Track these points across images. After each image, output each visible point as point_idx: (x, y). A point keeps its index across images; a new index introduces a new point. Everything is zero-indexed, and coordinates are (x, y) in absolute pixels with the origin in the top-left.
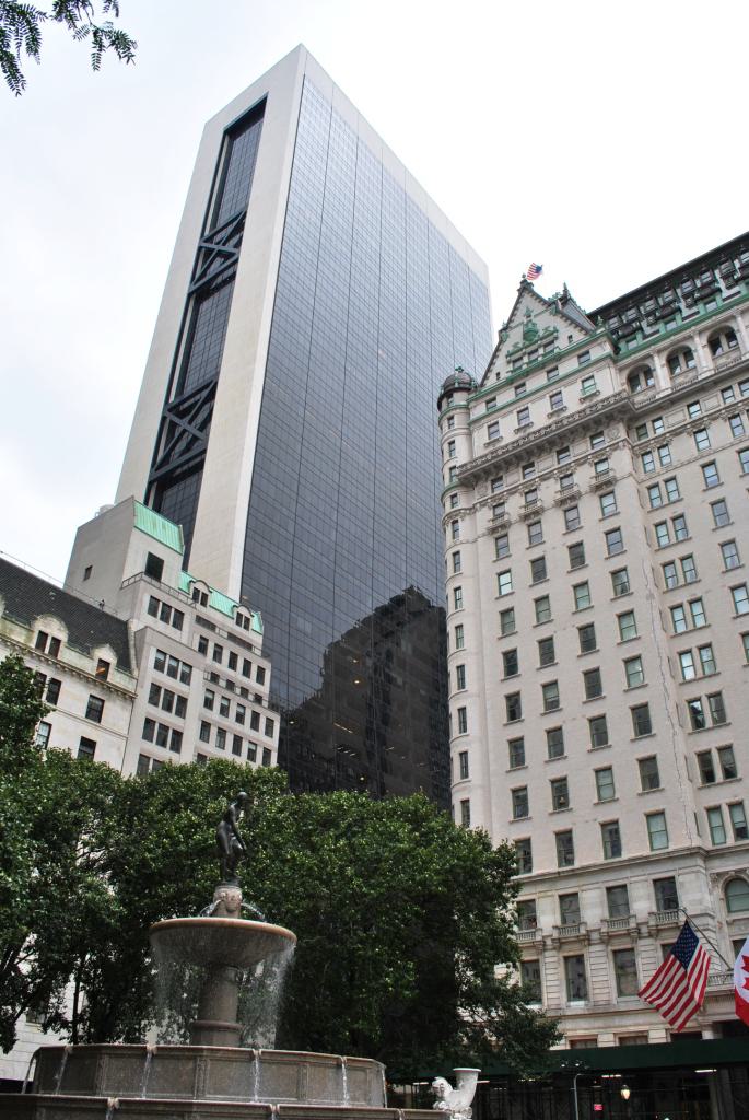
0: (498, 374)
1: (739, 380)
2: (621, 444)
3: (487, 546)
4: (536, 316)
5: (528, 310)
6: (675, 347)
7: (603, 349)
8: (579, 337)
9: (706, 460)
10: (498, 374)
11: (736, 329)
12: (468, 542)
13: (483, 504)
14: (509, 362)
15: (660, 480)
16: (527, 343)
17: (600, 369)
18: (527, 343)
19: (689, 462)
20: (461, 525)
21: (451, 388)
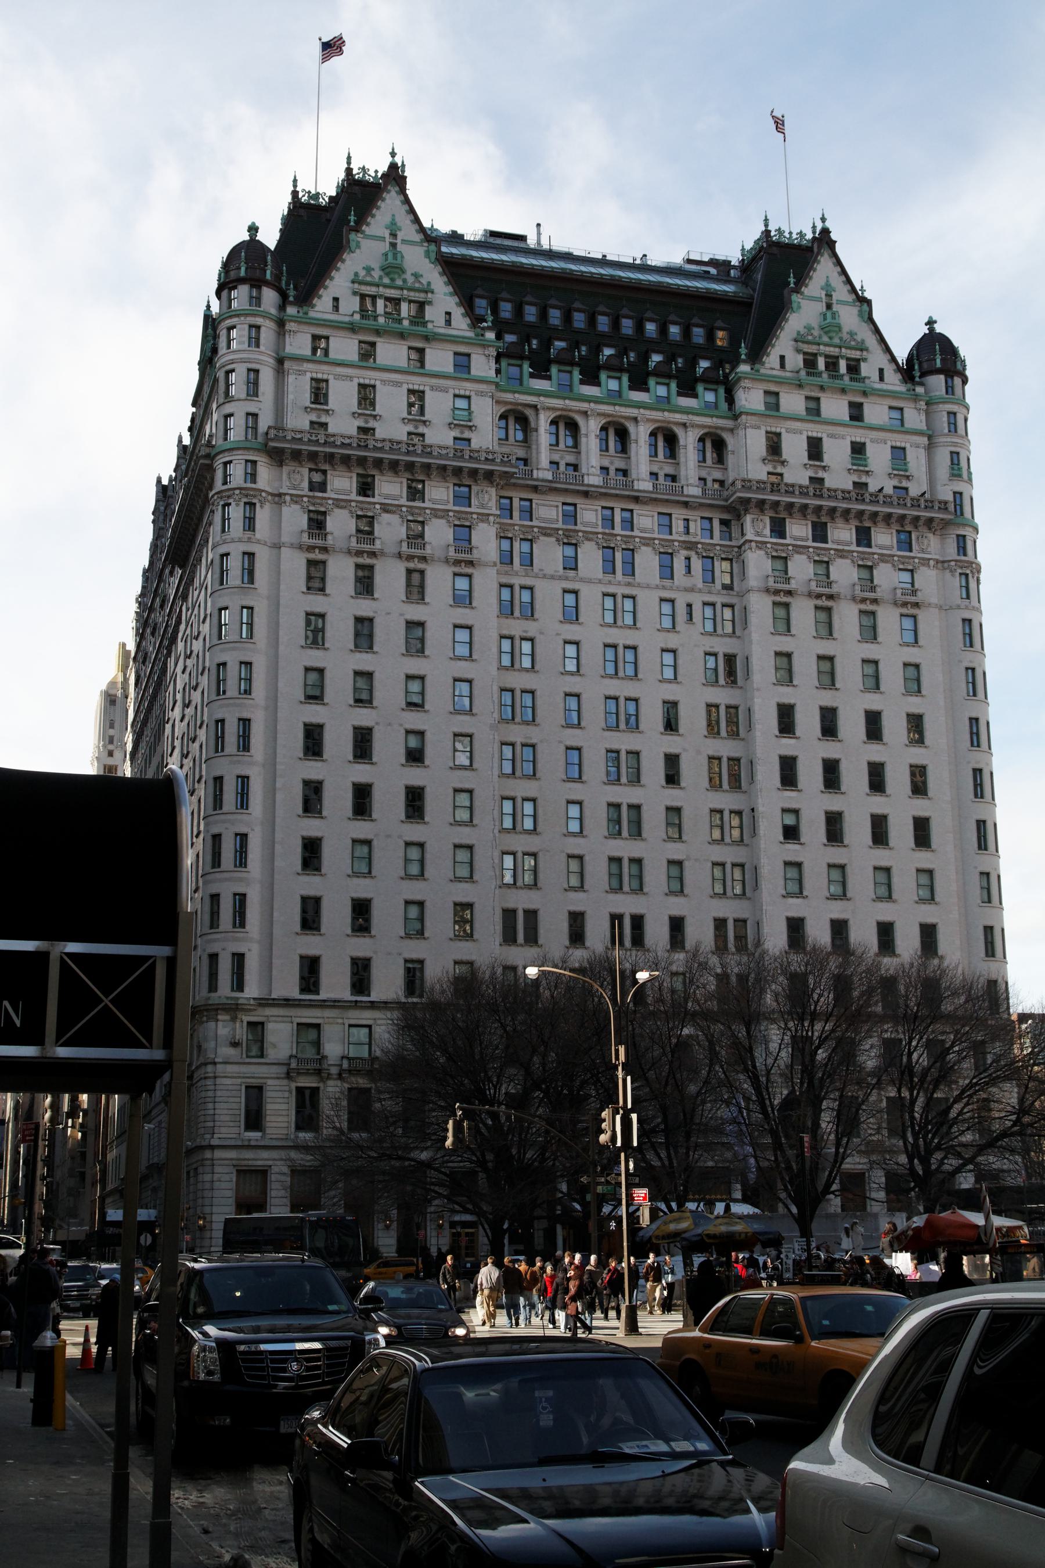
0: (336, 300)
1: (624, 507)
2: (491, 518)
3: (295, 564)
4: (404, 241)
5: (393, 223)
6: (564, 413)
7: (483, 365)
8: (461, 324)
9: (570, 586)
10: (336, 300)
11: (633, 436)
12: (265, 544)
13: (296, 499)
14: (355, 293)
15: (517, 581)
16: (386, 281)
17: (480, 394)
18: (386, 281)
19: (552, 577)
20: (263, 515)
21: (258, 273)
